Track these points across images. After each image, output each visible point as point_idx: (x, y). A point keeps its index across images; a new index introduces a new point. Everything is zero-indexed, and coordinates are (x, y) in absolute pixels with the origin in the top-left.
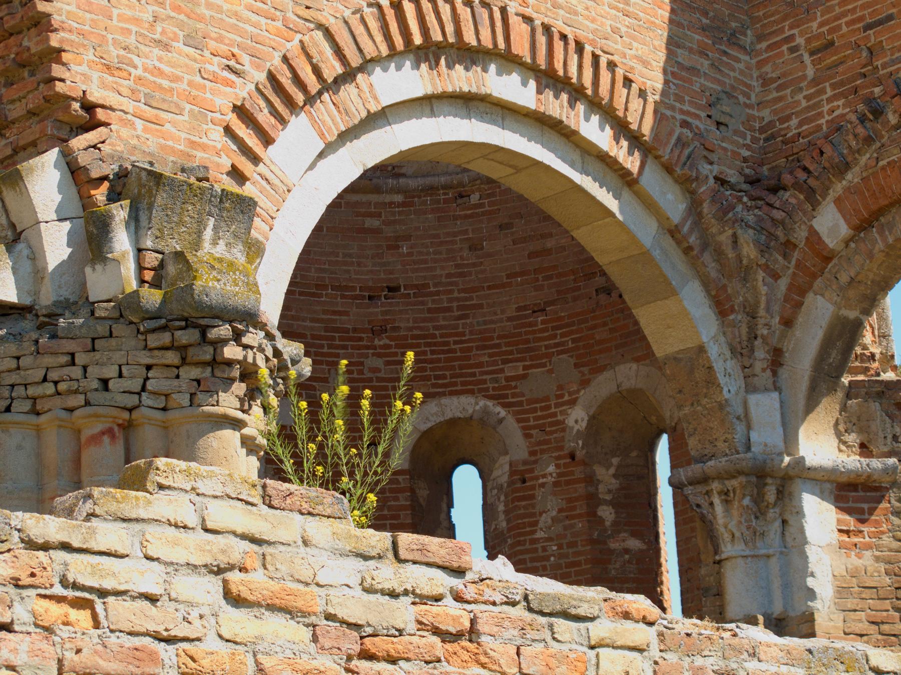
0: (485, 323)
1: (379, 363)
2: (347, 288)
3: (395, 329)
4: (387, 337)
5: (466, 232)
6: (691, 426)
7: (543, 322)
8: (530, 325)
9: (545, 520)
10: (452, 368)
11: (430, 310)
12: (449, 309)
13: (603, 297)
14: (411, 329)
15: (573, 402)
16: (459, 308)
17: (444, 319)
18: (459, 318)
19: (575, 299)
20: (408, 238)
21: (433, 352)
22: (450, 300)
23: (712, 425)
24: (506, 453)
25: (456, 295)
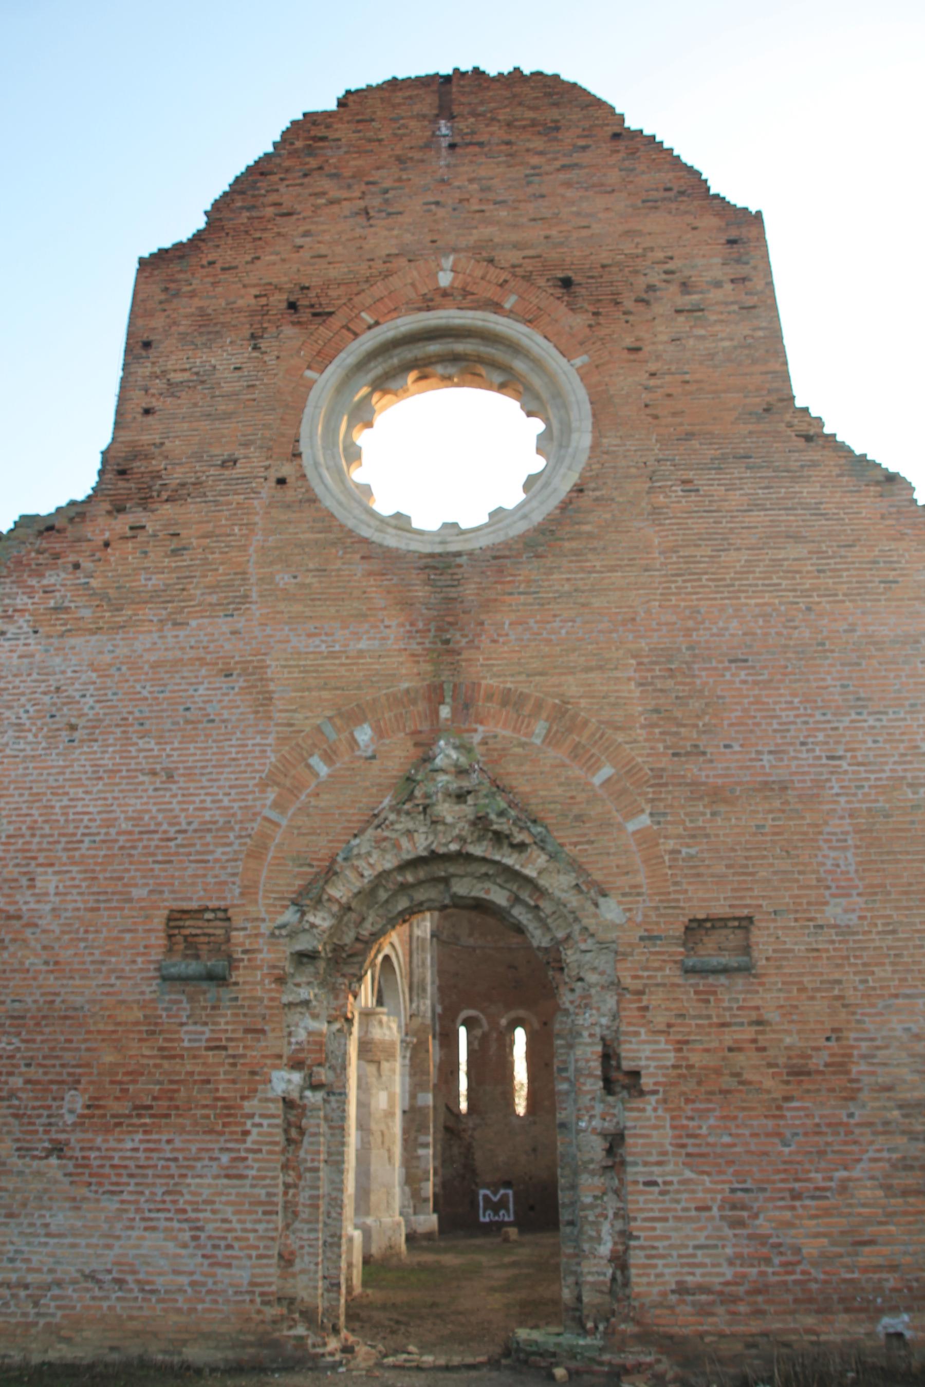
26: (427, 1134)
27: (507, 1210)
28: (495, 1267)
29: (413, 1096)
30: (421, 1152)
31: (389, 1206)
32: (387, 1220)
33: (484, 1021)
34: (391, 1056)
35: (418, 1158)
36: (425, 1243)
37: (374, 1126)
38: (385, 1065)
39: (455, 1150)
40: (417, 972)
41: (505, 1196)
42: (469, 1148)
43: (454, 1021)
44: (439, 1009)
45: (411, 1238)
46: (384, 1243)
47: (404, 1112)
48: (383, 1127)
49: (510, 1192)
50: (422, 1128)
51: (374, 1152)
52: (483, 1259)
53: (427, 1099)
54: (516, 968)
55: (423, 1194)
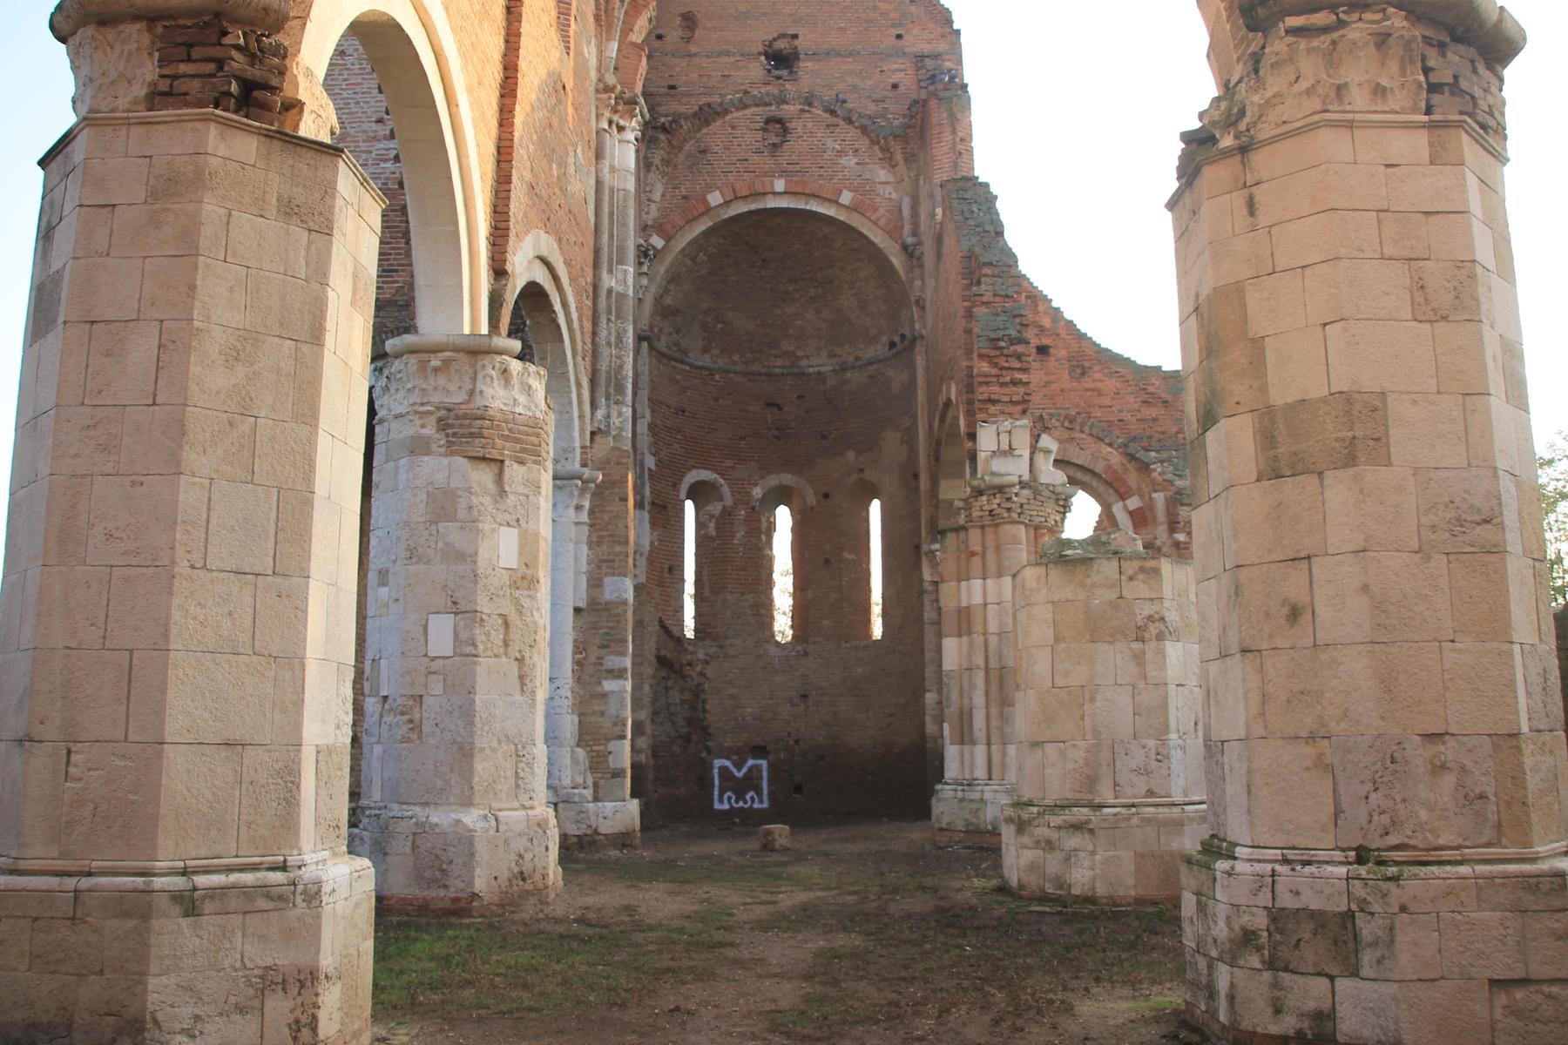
1: (676, 446)
9: (738, 535)
15: (756, 485)
24: (721, 499)
26: (624, 654)
27: (759, 792)
28: (765, 925)
29: (595, 583)
30: (609, 685)
31: (518, 783)
32: (513, 817)
33: (726, 491)
34: (528, 453)
35: (604, 696)
36: (614, 853)
37: (484, 605)
38: (513, 471)
39: (675, 697)
40: (605, 352)
41: (758, 768)
42: (697, 692)
43: (675, 486)
44: (650, 462)
45: (579, 850)
46: (505, 867)
47: (577, 610)
48: (508, 608)
49: (764, 763)
50: (612, 642)
51: (484, 665)
52: (729, 896)
53: (623, 589)
54: (780, 408)
55: (612, 762)
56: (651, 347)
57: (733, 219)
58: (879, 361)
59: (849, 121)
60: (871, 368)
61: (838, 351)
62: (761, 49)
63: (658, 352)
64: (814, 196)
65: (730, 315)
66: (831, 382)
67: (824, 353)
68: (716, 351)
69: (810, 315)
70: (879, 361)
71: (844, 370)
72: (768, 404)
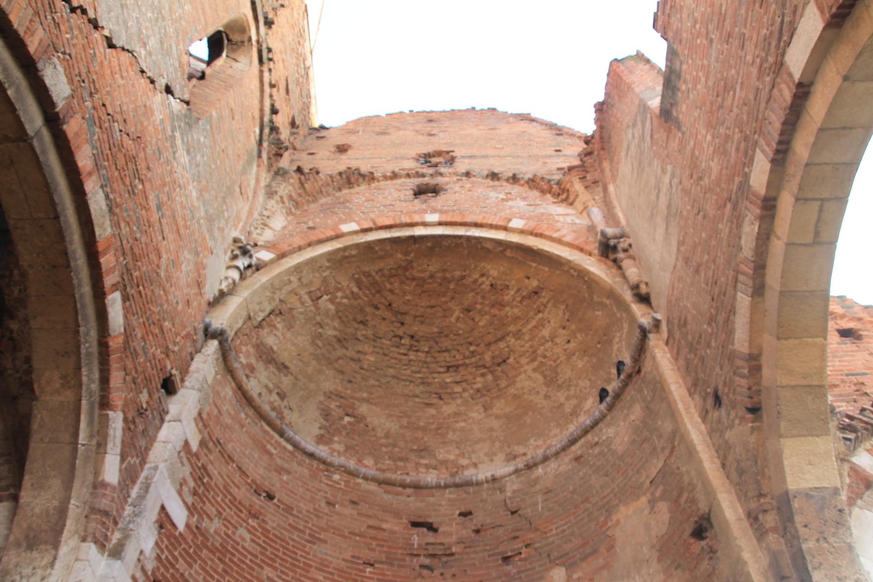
0: (326, 554)
2: (243, 472)
3: (264, 521)
4: (258, 524)
5: (326, 492)
6: (816, 560)
7: (370, 572)
8: (360, 570)
10: (295, 572)
11: (290, 525)
12: (303, 532)
13: (425, 572)
14: (274, 528)
16: (310, 535)
17: (298, 536)
18: (308, 541)
19: (400, 566)
20: (288, 472)
21: (284, 553)
22: (305, 526)
23: (840, 563)
25: (310, 525)
54: (431, 528)
56: (225, 353)
57: (369, 247)
58: (586, 431)
59: (514, 179)
60: (573, 448)
61: (521, 449)
62: (414, 156)
63: (240, 387)
64: (477, 225)
65: (363, 409)
66: (512, 486)
67: (501, 456)
68: (336, 446)
69: (477, 413)
70: (586, 431)
71: (530, 467)
72: (415, 524)
